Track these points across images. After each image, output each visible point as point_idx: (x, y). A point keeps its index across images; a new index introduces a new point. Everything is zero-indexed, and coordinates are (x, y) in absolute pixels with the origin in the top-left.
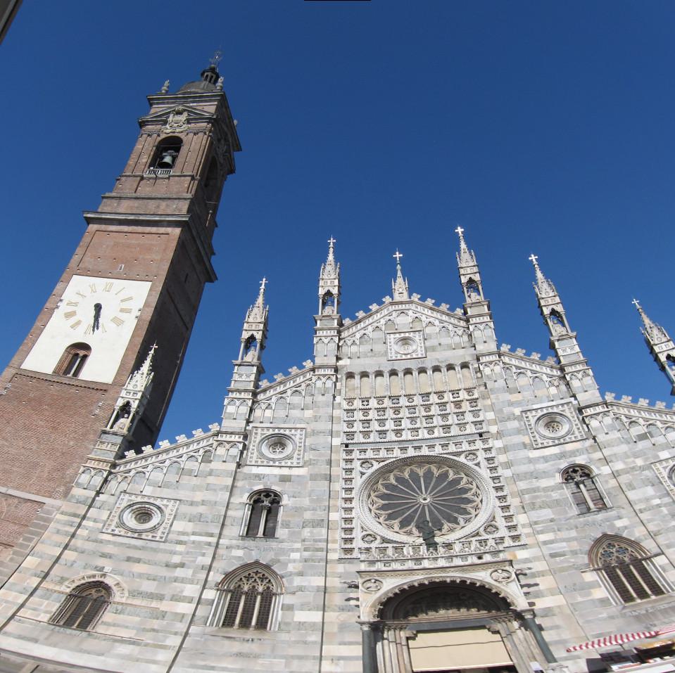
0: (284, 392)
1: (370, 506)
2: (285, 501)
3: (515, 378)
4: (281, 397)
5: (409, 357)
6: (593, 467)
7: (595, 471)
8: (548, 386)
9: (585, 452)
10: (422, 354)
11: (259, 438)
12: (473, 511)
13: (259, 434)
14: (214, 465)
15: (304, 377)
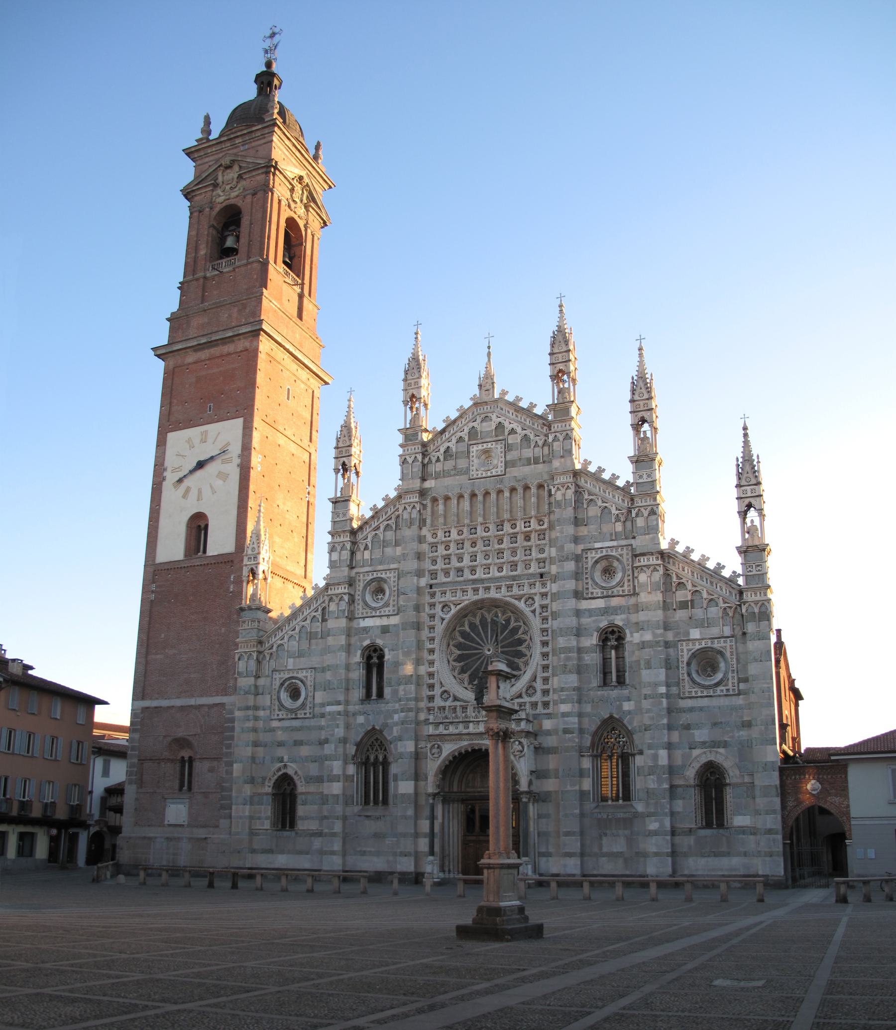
0: (378, 528)
1: (449, 657)
2: (387, 657)
3: (585, 506)
4: (376, 534)
5: (489, 474)
6: (627, 631)
7: (628, 638)
8: (613, 520)
9: (626, 611)
10: (502, 471)
11: (362, 585)
12: (522, 667)
13: (362, 581)
14: (331, 624)
15: (395, 506)
